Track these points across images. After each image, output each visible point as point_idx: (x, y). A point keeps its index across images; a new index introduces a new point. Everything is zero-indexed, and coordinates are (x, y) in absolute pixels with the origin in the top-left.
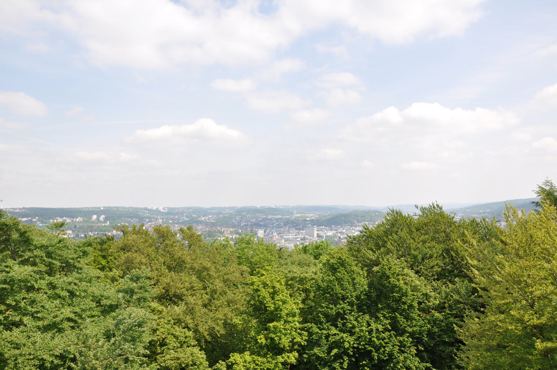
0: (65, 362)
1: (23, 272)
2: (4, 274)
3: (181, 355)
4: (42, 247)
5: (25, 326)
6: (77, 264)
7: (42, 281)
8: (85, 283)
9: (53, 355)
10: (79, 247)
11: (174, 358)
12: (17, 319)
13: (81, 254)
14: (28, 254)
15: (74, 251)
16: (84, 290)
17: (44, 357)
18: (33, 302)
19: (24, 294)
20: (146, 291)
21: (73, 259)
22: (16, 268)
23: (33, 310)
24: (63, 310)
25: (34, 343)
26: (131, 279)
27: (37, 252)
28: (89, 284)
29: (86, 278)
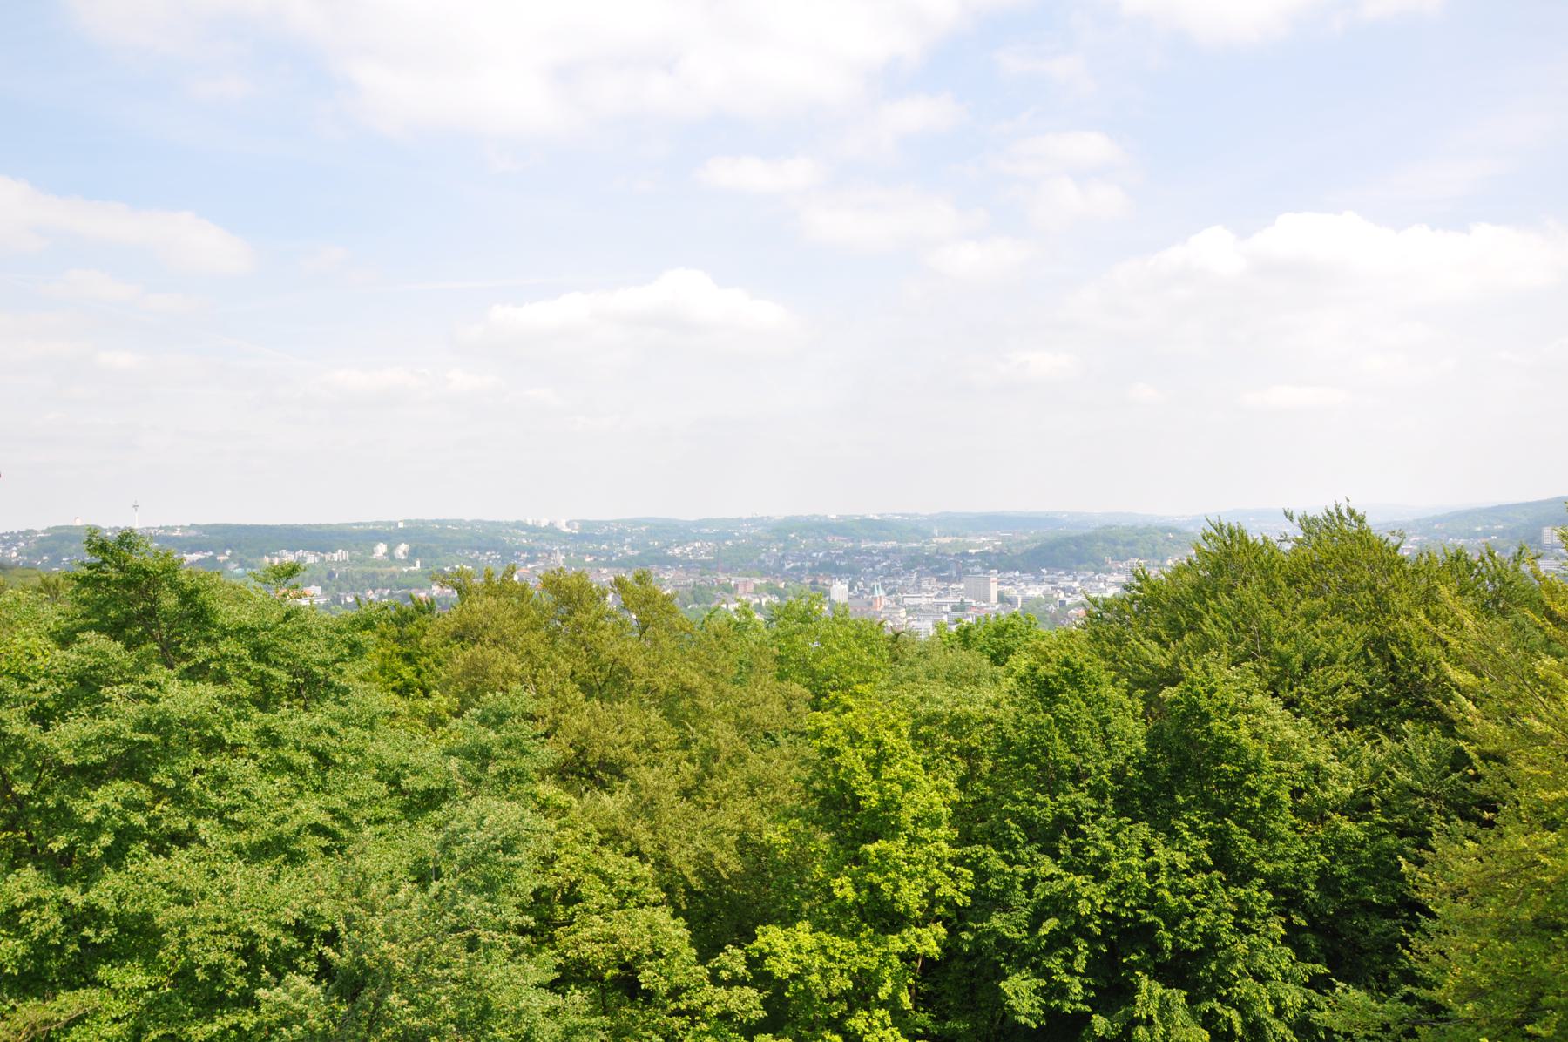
0: (309, 943)
2: (143, 704)
3: (621, 930)
4: (241, 631)
5: (204, 843)
6: (333, 678)
7: (243, 725)
9: (278, 923)
10: (339, 631)
12: (182, 825)
13: (346, 651)
14: (203, 652)
15: (326, 642)
16: (357, 750)
17: (254, 927)
18: (221, 780)
19: (195, 758)
20: (523, 752)
21: (323, 664)
22: (174, 688)
23: (223, 802)
24: (299, 804)
25: (228, 891)
26: (483, 721)
27: (228, 646)
28: (367, 734)
29: (359, 716)
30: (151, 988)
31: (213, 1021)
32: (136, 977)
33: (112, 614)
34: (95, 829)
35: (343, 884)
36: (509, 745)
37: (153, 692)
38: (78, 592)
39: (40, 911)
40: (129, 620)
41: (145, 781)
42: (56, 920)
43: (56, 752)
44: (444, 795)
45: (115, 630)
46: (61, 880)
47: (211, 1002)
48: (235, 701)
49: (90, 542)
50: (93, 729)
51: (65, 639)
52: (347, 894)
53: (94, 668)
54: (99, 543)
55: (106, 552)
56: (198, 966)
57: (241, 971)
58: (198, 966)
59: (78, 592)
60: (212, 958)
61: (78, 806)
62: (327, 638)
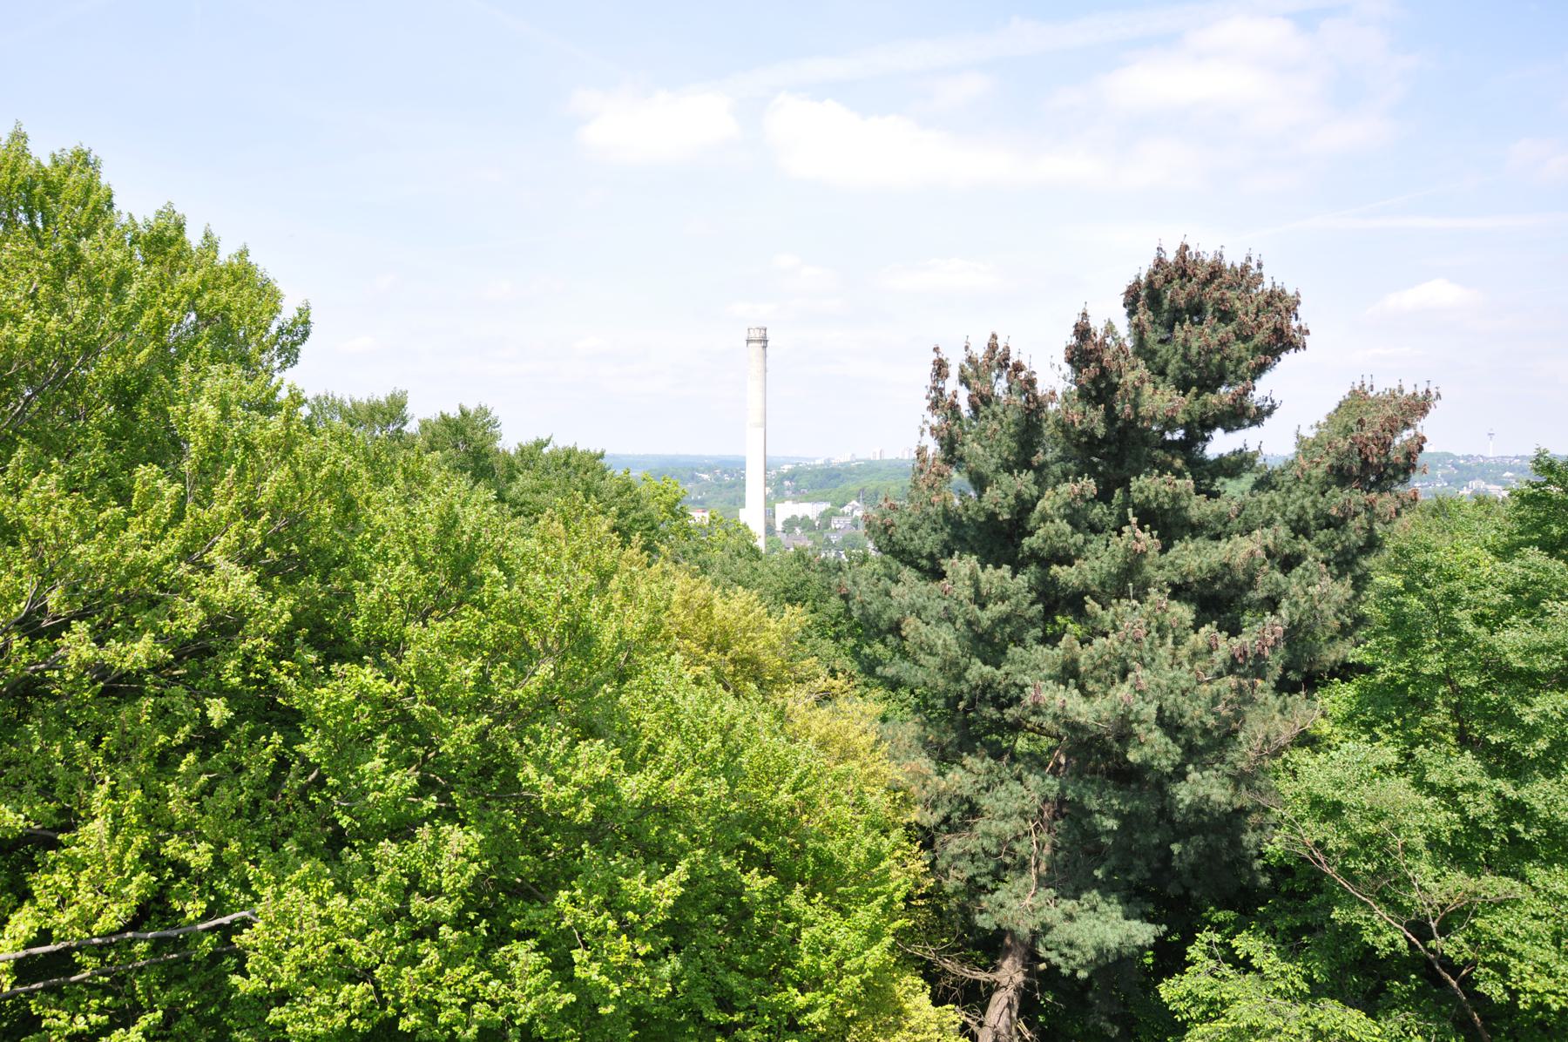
34: (1532, 733)
39: (1475, 795)
42: (1489, 807)
43: (1505, 653)
46: (1494, 773)
49: (1537, 461)
50: (1540, 638)
51: (1506, 553)
53: (1536, 583)
54: (1546, 463)
59: (1518, 509)
61: (1518, 709)
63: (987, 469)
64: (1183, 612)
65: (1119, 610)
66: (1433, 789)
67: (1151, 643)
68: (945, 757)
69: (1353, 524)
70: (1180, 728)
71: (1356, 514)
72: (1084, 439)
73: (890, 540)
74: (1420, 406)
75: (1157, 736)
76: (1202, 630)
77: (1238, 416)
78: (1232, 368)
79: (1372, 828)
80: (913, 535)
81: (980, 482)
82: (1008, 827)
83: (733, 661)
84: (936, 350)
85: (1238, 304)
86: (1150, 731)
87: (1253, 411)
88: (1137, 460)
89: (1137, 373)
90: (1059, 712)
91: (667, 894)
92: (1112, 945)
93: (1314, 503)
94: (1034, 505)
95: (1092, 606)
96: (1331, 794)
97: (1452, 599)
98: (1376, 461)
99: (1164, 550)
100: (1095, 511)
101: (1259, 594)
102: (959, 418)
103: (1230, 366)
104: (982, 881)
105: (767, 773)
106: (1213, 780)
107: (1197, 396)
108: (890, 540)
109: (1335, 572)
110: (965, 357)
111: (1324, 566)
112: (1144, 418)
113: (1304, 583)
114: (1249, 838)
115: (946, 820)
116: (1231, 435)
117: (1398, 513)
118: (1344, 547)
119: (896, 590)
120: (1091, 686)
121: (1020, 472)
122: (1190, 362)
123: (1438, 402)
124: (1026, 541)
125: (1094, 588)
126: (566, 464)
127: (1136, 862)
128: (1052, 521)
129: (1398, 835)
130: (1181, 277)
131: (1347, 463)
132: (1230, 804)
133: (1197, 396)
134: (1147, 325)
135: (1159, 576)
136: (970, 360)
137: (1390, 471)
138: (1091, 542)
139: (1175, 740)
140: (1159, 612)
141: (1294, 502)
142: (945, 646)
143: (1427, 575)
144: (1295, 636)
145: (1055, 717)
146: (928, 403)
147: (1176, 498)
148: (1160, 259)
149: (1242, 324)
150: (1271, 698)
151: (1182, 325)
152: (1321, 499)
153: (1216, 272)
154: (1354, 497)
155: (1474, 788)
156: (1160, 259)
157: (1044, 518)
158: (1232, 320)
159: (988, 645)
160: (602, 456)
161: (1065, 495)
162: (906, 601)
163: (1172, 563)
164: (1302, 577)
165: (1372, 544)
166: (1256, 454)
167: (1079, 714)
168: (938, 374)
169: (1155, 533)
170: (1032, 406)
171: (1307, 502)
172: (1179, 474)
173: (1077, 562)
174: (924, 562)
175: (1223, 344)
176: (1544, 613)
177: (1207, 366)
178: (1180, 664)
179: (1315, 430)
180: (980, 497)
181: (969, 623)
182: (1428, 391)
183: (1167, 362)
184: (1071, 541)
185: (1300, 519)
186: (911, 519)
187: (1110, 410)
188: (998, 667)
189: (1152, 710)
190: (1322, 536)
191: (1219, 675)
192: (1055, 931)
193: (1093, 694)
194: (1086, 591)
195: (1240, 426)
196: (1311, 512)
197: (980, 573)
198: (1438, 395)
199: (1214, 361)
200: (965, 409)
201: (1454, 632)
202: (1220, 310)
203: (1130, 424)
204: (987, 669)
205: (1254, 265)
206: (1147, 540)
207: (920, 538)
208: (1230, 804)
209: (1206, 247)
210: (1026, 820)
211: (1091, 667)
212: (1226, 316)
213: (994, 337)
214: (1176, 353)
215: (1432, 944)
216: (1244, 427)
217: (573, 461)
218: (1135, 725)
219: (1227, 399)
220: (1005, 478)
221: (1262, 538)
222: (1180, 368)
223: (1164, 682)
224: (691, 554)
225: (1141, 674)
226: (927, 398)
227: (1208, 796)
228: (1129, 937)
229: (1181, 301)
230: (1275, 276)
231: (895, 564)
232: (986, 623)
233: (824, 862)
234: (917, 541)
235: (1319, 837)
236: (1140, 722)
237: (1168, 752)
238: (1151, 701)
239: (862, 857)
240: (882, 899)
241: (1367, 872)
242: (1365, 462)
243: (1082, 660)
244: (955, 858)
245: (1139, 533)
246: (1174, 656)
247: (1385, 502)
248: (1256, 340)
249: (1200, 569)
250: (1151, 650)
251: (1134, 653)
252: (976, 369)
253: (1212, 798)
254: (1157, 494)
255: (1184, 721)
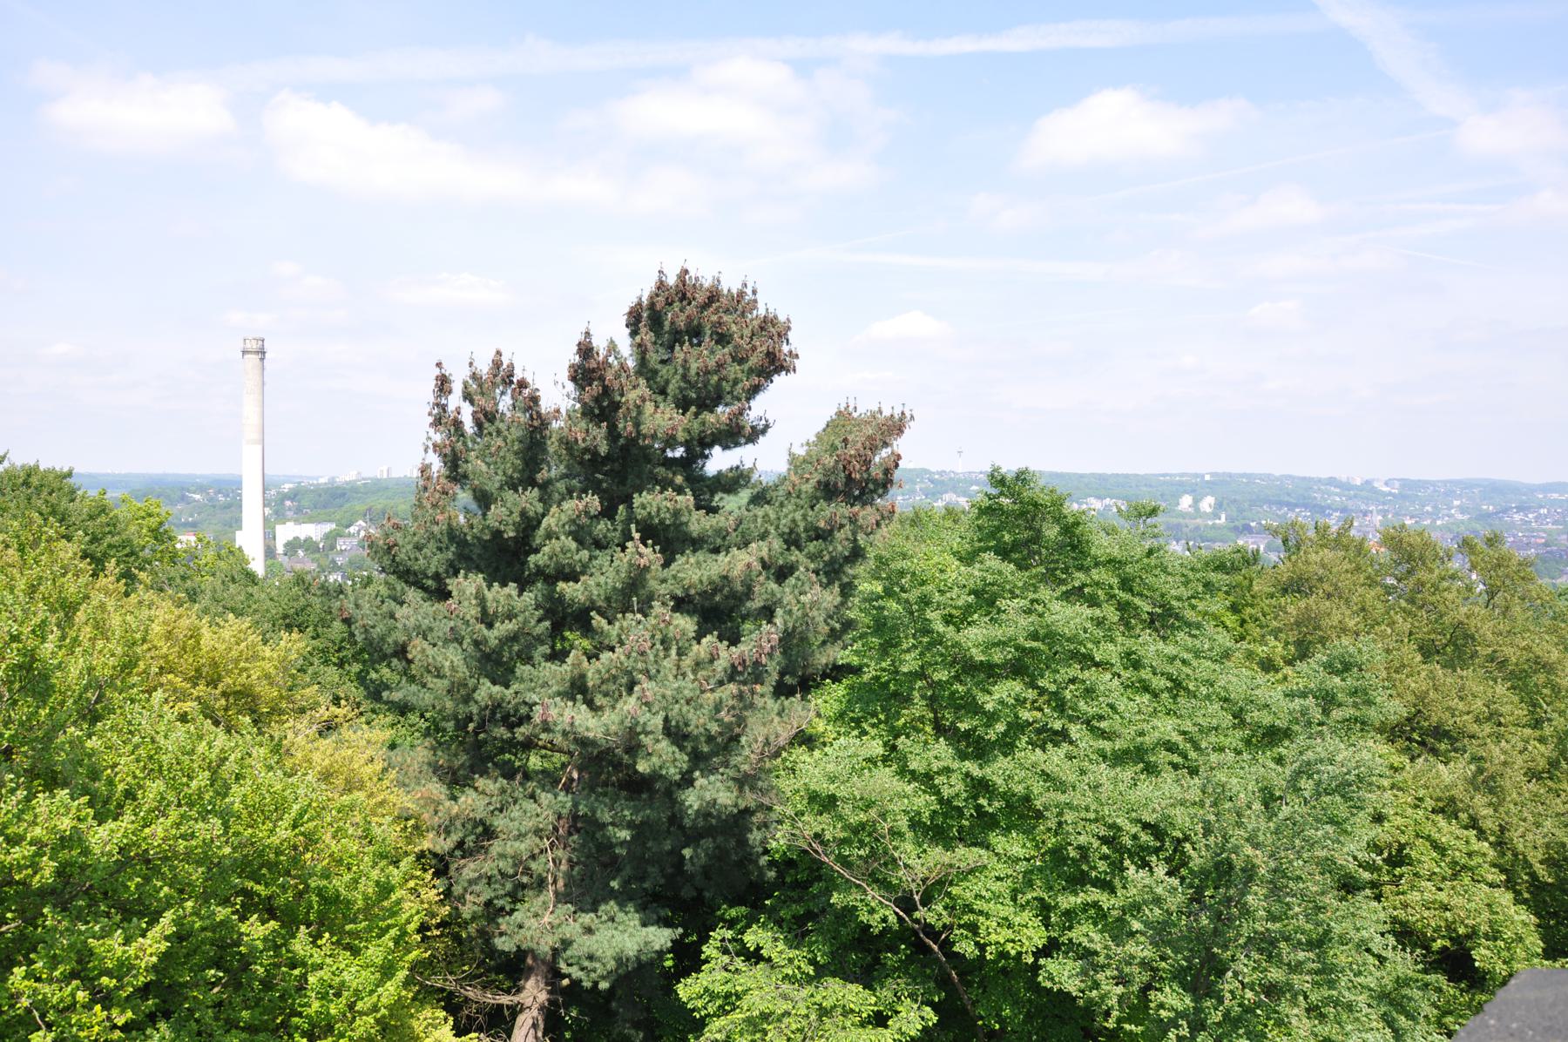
0: (1163, 841)
1: (1072, 618)
2: (1033, 618)
3: (1457, 901)
4: (1113, 563)
5: (1071, 743)
6: (1189, 615)
7: (1111, 647)
8: (1209, 663)
9: (1140, 821)
10: (1192, 569)
11: (1433, 902)
12: (1057, 725)
13: (1200, 589)
14: (1079, 578)
15: (1183, 579)
16: (1207, 681)
17: (1118, 821)
18: (1089, 693)
19: (1074, 671)
20: (1369, 703)
21: (1179, 599)
22: (1056, 606)
23: (1091, 711)
24: (1155, 722)
25: (1095, 787)
26: (1330, 668)
27: (1097, 575)
28: (1217, 667)
29: (1211, 650)
30: (1026, 859)
31: (1076, 894)
32: (1014, 845)
33: (1007, 537)
34: (992, 718)
35: (1204, 793)
36: (1354, 693)
37: (1040, 608)
38: (977, 519)
39: (948, 777)
40: (1016, 546)
41: (1033, 685)
42: (960, 787)
44: (1287, 734)
45: (1004, 553)
46: (963, 756)
47: (1078, 881)
48: (1099, 622)
49: (992, 476)
50: (998, 633)
51: (968, 559)
52: (1208, 802)
55: (1004, 486)
56: (1071, 845)
57: (1104, 857)
58: (1071, 845)
59: (977, 519)
60: (1082, 840)
61: (981, 698)
62: (1183, 575)
63: (492, 486)
64: (686, 624)
65: (625, 624)
66: (914, 776)
67: (656, 656)
68: (456, 780)
69: (839, 535)
70: (686, 737)
71: (842, 526)
72: (587, 457)
73: (393, 561)
74: (896, 427)
75: (665, 746)
76: (704, 641)
77: (734, 435)
78: (728, 389)
79: (863, 817)
80: (418, 554)
81: (484, 500)
82: (523, 847)
83: (224, 694)
84: (439, 365)
85: (734, 328)
86: (658, 741)
87: (748, 430)
88: (639, 476)
89: (638, 392)
90: (568, 729)
91: (148, 952)
92: (631, 954)
93: (804, 517)
94: (540, 523)
95: (598, 621)
96: (825, 788)
97: (925, 601)
98: (858, 476)
99: (666, 565)
100: (599, 527)
101: (756, 604)
102: (463, 435)
103: (726, 386)
104: (499, 903)
105: (262, 811)
106: (719, 784)
107: (696, 415)
108: (393, 561)
109: (825, 580)
110: (469, 373)
111: (814, 576)
112: (645, 437)
113: (796, 592)
114: (755, 837)
115: (460, 845)
116: (728, 452)
117: (878, 524)
118: (832, 557)
119: (400, 612)
120: (599, 700)
121: (525, 489)
122: (689, 382)
123: (911, 424)
124: (532, 558)
125: (600, 603)
126: (26, 484)
127: (650, 869)
128: (558, 538)
129: (885, 820)
130: (681, 300)
131: (832, 478)
132: (736, 805)
133: (696, 415)
134: (649, 345)
135: (663, 590)
136: (474, 376)
137: (871, 486)
138: (596, 558)
139: (681, 748)
140: (662, 625)
141: (786, 516)
142: (453, 668)
143: (903, 581)
144: (792, 642)
145: (565, 734)
146: (431, 419)
147: (677, 513)
148: (661, 282)
149: (737, 347)
150: (770, 703)
151: (681, 346)
152: (811, 513)
153: (713, 296)
154: (839, 510)
155: (947, 771)
156: (661, 282)
157: (550, 535)
158: (728, 343)
159: (496, 665)
160: (70, 474)
161: (570, 512)
162: (411, 622)
163: (674, 577)
164: (795, 586)
165: (857, 554)
166: (751, 470)
167: (588, 729)
168: (441, 390)
169: (657, 548)
170: (536, 423)
171: (798, 516)
172: (679, 490)
173: (582, 578)
174: (430, 582)
175: (720, 365)
176: (999, 611)
177: (705, 386)
178: (684, 675)
179: (806, 448)
180: (484, 515)
181: (476, 643)
182: (903, 413)
183: (667, 382)
184: (577, 558)
185: (791, 531)
186: (416, 539)
187: (612, 428)
188: (507, 687)
189: (657, 722)
190: (812, 547)
191: (721, 683)
192: (575, 945)
193: (601, 708)
194: (593, 606)
195: (737, 444)
196: (802, 525)
197: (486, 592)
198: (912, 417)
199: (712, 382)
200: (469, 426)
201: (927, 631)
202: (718, 333)
203: (632, 442)
204: (497, 689)
205: (749, 291)
206: (649, 555)
207: (425, 558)
208: (736, 805)
209: (705, 272)
210: (541, 838)
211: (598, 682)
212: (722, 339)
213: (499, 353)
214: (676, 373)
215: (917, 915)
216: (740, 445)
217: (35, 481)
218: (642, 736)
219: (724, 418)
220: (509, 495)
221: (759, 550)
222: (680, 388)
223: (669, 693)
224: (178, 580)
225: (647, 687)
226: (430, 414)
227: (715, 800)
228: (646, 943)
229: (681, 324)
230: (769, 303)
231: (400, 585)
232: (493, 642)
233: (331, 900)
234: (422, 561)
235: (818, 829)
236: (647, 734)
237: (675, 760)
238: (658, 712)
239: (370, 890)
240: (393, 932)
241: (860, 857)
242: (849, 477)
243: (590, 675)
244: (471, 882)
245: (642, 548)
246: (679, 667)
247: (867, 515)
248: (750, 363)
249: (701, 582)
250: (656, 662)
251: (640, 666)
252: (480, 386)
253: (719, 801)
254: (659, 509)
255: (690, 729)
